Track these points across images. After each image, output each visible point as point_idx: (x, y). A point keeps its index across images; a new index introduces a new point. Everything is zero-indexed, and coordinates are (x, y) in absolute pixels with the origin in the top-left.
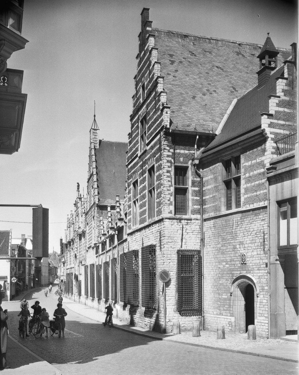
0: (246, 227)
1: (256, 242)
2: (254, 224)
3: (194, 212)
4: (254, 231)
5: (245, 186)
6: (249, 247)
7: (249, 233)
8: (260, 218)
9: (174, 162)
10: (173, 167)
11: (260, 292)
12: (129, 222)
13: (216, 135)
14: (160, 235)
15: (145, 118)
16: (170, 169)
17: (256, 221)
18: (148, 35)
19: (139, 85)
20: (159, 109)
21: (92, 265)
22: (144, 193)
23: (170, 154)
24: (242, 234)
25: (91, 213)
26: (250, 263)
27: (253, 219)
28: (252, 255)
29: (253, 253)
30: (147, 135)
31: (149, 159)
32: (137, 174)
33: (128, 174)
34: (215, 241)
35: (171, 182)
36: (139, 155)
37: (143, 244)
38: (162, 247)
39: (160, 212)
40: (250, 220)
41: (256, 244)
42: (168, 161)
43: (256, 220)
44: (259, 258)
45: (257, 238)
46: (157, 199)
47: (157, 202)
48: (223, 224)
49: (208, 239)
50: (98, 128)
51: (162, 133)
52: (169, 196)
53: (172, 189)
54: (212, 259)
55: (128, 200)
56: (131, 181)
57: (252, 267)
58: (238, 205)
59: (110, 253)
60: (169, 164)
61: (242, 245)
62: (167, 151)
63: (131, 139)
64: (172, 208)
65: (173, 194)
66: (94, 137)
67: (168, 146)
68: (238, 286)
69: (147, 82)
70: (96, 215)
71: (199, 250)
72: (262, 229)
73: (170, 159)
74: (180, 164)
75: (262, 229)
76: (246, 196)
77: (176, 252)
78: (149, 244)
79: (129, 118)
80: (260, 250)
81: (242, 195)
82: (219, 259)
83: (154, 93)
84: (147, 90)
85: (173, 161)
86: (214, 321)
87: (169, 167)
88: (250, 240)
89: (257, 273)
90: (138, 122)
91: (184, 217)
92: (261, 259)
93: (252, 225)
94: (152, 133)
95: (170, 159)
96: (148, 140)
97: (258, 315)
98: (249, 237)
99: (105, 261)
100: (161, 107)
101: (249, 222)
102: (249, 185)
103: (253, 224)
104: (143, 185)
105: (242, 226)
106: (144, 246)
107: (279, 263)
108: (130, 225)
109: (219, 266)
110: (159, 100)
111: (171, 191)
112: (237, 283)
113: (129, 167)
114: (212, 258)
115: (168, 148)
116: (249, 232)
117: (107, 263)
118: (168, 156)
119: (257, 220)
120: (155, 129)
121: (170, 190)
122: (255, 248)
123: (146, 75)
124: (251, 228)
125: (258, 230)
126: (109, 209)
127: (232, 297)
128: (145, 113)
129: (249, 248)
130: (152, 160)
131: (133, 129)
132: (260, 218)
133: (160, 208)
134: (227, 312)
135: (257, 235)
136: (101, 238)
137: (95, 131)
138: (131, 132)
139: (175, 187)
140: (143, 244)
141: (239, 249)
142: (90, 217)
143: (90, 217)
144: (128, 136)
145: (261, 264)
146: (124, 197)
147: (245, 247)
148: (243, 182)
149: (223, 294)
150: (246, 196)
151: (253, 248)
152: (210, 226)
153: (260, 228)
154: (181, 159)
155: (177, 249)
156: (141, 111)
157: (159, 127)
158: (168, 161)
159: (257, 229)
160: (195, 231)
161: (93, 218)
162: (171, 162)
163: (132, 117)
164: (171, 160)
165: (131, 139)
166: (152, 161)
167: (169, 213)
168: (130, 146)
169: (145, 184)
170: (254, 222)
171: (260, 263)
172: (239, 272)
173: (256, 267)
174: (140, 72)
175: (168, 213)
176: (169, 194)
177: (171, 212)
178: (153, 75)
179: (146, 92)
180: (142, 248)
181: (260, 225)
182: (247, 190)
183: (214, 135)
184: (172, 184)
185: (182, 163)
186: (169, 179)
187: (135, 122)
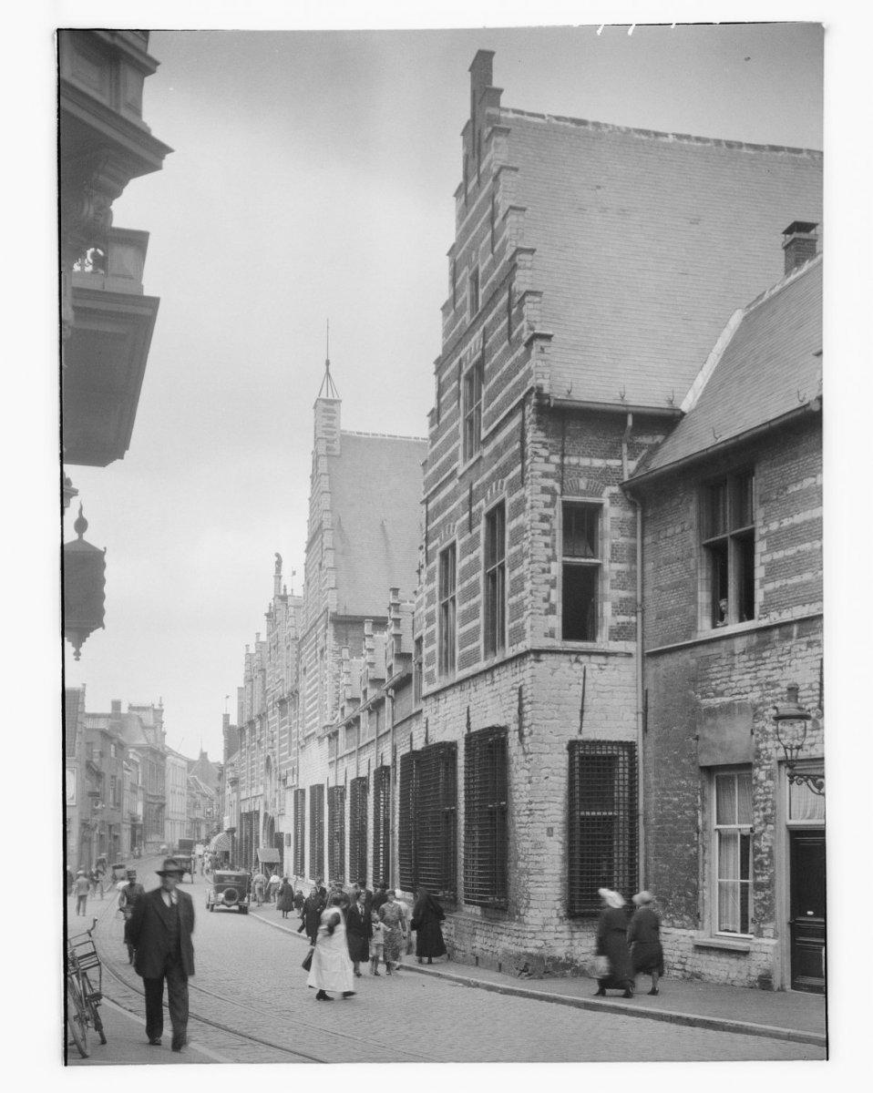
2: (793, 668)
3: (620, 633)
5: (767, 558)
9: (562, 490)
10: (558, 509)
12: (428, 665)
13: (683, 414)
14: (520, 699)
15: (479, 366)
16: (550, 511)
18: (490, 129)
19: (463, 274)
21: (317, 790)
22: (473, 578)
23: (551, 468)
25: (317, 638)
30: (483, 415)
31: (487, 484)
32: (454, 527)
33: (427, 524)
35: (553, 547)
36: (460, 472)
37: (469, 724)
38: (526, 731)
39: (519, 634)
42: (545, 490)
46: (511, 596)
47: (513, 607)
50: (336, 398)
51: (529, 410)
53: (556, 569)
55: (426, 600)
56: (436, 547)
58: (747, 611)
59: (370, 754)
60: (548, 498)
62: (542, 460)
63: (436, 426)
64: (556, 622)
65: (559, 582)
66: (325, 422)
67: (544, 445)
69: (486, 264)
70: (331, 642)
71: (631, 743)
73: (550, 483)
76: (770, 587)
77: (565, 746)
78: (488, 724)
79: (433, 368)
81: (757, 584)
83: (506, 296)
84: (485, 288)
85: (557, 487)
87: (547, 505)
90: (459, 379)
94: (499, 409)
95: (550, 483)
96: (487, 429)
99: (354, 777)
100: (526, 336)
102: (778, 555)
104: (472, 557)
105: (755, 672)
106: (472, 731)
108: (432, 672)
110: (520, 316)
111: (553, 572)
113: (431, 505)
115: (544, 452)
117: (360, 784)
118: (546, 475)
120: (509, 398)
121: (549, 572)
123: (482, 245)
126: (367, 629)
128: (479, 354)
130: (497, 484)
131: (442, 399)
136: (343, 709)
137: (331, 407)
138: (436, 407)
139: (563, 562)
140: (469, 724)
142: (311, 652)
143: (311, 652)
144: (428, 419)
146: (415, 592)
148: (760, 547)
150: (770, 587)
154: (583, 484)
155: (568, 739)
156: (467, 348)
157: (519, 392)
158: (545, 490)
161: (322, 651)
163: (440, 364)
164: (553, 488)
165: (436, 426)
166: (496, 488)
167: (546, 635)
168: (435, 447)
169: (475, 553)
174: (462, 237)
175: (543, 635)
176: (547, 582)
177: (551, 635)
178: (504, 243)
179: (481, 292)
180: (469, 738)
183: (677, 413)
185: (584, 493)
186: (548, 539)
187: (448, 378)
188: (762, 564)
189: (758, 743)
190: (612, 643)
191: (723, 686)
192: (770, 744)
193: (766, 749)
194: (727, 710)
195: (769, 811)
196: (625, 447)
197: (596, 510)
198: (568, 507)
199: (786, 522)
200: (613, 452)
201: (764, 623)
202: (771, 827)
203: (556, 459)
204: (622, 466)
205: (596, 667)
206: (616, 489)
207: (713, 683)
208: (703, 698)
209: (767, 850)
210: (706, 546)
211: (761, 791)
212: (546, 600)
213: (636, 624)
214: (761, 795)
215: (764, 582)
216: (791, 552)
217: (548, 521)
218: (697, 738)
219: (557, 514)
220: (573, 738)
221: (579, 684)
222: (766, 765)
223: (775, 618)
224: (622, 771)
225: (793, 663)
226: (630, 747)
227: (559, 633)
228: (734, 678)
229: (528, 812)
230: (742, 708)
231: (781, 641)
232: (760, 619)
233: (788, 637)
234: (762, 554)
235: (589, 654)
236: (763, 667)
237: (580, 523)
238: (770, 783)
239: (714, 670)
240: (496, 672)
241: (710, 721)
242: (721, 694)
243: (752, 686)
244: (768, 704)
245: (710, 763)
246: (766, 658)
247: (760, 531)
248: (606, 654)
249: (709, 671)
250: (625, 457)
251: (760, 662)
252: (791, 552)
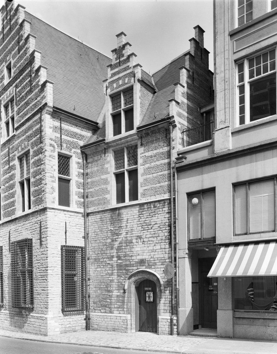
0: (145, 221)
1: (159, 236)
4: (156, 224)
6: (149, 241)
7: (149, 226)
8: (165, 211)
11: (165, 287)
17: (159, 214)
24: (140, 228)
26: (151, 258)
27: (155, 212)
28: (153, 249)
29: (155, 247)
34: (102, 236)
40: (151, 213)
41: (159, 238)
42: (51, 145)
43: (158, 213)
44: (164, 252)
45: (161, 231)
48: (114, 217)
49: (93, 234)
54: (98, 255)
57: (154, 262)
58: (134, 195)
60: (52, 148)
61: (139, 240)
68: (134, 282)
72: (167, 222)
75: (167, 222)
80: (164, 244)
82: (108, 255)
86: (102, 320)
88: (150, 234)
89: (161, 268)
92: (165, 253)
93: (154, 218)
97: (162, 311)
98: (149, 231)
101: (150, 215)
103: (155, 216)
105: (139, 219)
107: (187, 257)
109: (108, 262)
112: (133, 279)
114: (98, 254)
116: (150, 225)
119: (161, 212)
122: (157, 242)
124: (151, 221)
125: (162, 223)
127: (126, 294)
129: (149, 242)
132: (165, 211)
133: (40, 196)
134: (119, 309)
135: (160, 228)
139: (58, 176)
141: (135, 244)
145: (165, 258)
147: (144, 242)
149: (114, 291)
151: (155, 242)
152: (96, 220)
153: (164, 222)
158: (51, 145)
159: (161, 222)
160: (78, 225)
170: (157, 215)
171: (164, 257)
172: (135, 268)
173: (159, 262)
181: (165, 218)
224: (79, 256)
236: (142, 217)
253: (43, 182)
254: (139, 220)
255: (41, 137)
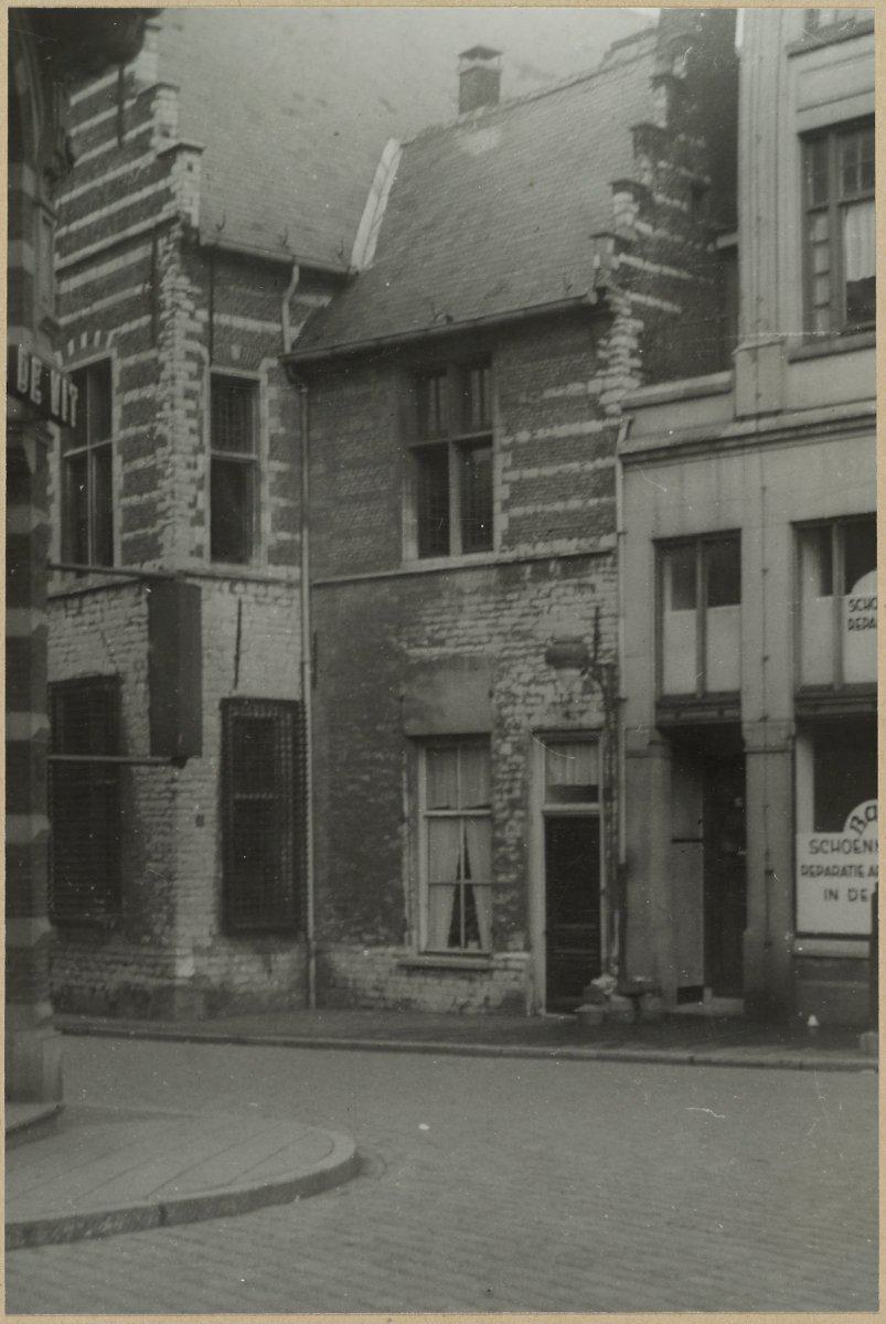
5: (513, 476)
9: (211, 360)
10: (206, 379)
16: (195, 385)
20: (141, 145)
35: (201, 436)
42: (190, 355)
47: (130, 511)
52: (192, 489)
53: (204, 462)
58: (479, 537)
60: (193, 366)
64: (203, 535)
65: (207, 482)
67: (189, 295)
73: (196, 347)
74: (229, 371)
76: (517, 511)
77: (217, 704)
81: (497, 507)
85: (205, 352)
87: (192, 377)
91: (241, 570)
105: (497, 618)
115: (189, 305)
118: (190, 335)
121: (195, 466)
133: (150, 531)
139: (212, 456)
150: (517, 511)
154: (236, 351)
158: (190, 355)
162: (200, 362)
164: (199, 355)
167: (192, 553)
176: (192, 481)
177: (198, 552)
182: (520, 491)
184: (201, 442)
185: (232, 363)
186: (193, 423)
188: (504, 482)
189: (500, 707)
190: (271, 567)
191: (444, 634)
192: (519, 709)
193: (512, 715)
194: (454, 662)
195: (517, 794)
196: (285, 307)
197: (248, 388)
198: (218, 382)
199: (542, 434)
200: (269, 313)
201: (509, 556)
202: (519, 813)
203: (203, 314)
204: (282, 331)
205: (252, 599)
206: (274, 363)
207: (428, 629)
208: (409, 647)
209: (514, 841)
210: (412, 450)
211: (505, 768)
212: (192, 505)
213: (301, 542)
214: (504, 773)
215: (506, 505)
216: (549, 471)
217: (193, 399)
218: (401, 699)
219: (203, 387)
220: (227, 695)
221: (232, 622)
222: (512, 735)
223: (524, 550)
225: (555, 609)
226: (294, 707)
227: (207, 550)
228: (460, 624)
229: (168, 795)
230: (474, 664)
231: (534, 580)
232: (503, 551)
233: (547, 576)
234: (505, 470)
235: (245, 581)
236: (506, 612)
237: (230, 401)
238: (519, 758)
239: (429, 612)
240: (88, 600)
241: (422, 677)
242: (441, 643)
243: (491, 635)
244: (517, 658)
245: (418, 732)
246: (511, 601)
247: (501, 439)
248: (266, 582)
249: (421, 612)
250: (286, 321)
251: (503, 606)
252: (549, 471)
253: (165, 484)
254: (494, 621)
255: (155, 328)
